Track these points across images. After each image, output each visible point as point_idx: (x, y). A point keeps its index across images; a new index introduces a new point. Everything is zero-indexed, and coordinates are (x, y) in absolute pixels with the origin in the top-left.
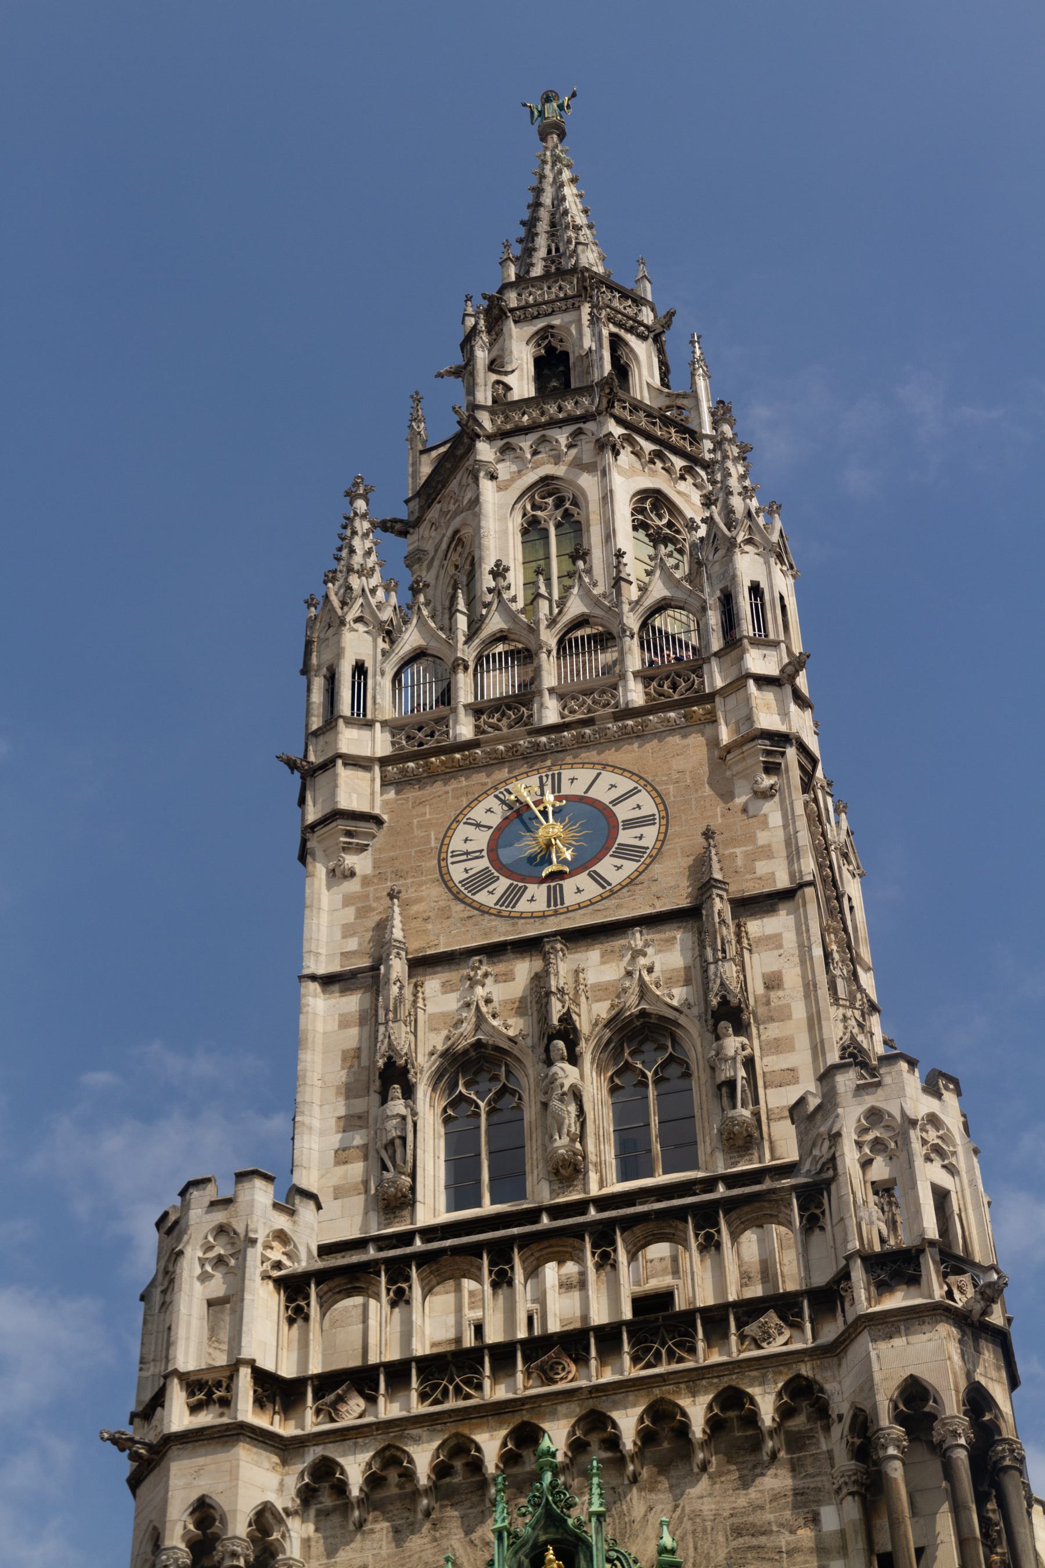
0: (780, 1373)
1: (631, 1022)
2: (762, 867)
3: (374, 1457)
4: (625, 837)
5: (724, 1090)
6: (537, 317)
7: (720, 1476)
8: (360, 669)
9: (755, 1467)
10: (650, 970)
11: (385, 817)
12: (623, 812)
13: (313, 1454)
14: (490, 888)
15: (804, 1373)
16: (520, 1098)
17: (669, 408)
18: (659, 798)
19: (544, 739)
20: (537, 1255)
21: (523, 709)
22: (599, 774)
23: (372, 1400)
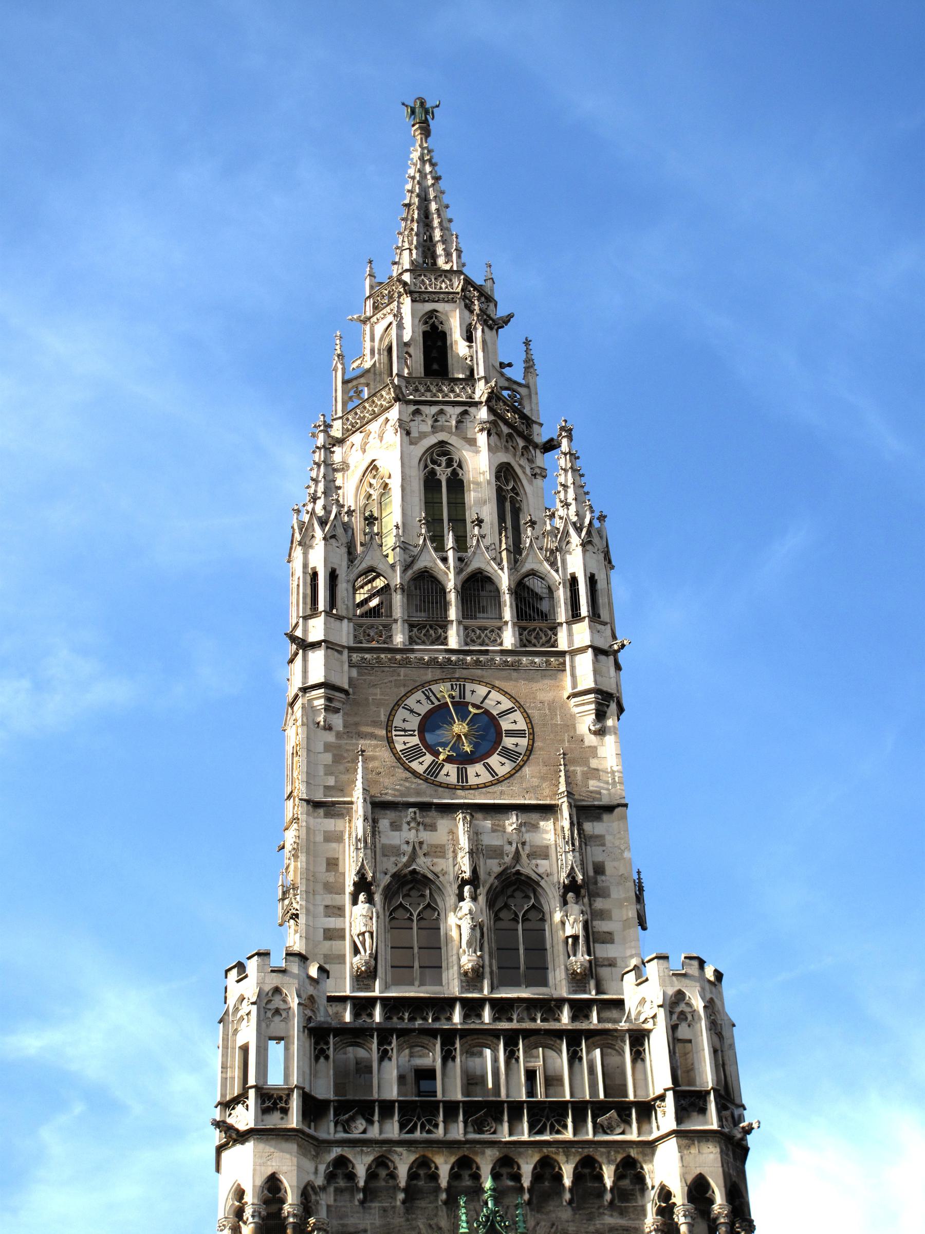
0: (618, 1152)
1: (509, 877)
2: (593, 784)
3: (373, 1161)
4: (508, 742)
5: (570, 940)
6: (427, 301)
7: (579, 1210)
8: (333, 577)
9: (599, 1208)
10: (524, 844)
11: (351, 691)
12: (505, 725)
13: (336, 1152)
14: (421, 760)
15: (632, 1155)
16: (439, 915)
17: (506, 389)
18: (528, 718)
19: (454, 658)
20: (470, 1042)
21: (440, 631)
22: (490, 692)
23: (370, 1122)
